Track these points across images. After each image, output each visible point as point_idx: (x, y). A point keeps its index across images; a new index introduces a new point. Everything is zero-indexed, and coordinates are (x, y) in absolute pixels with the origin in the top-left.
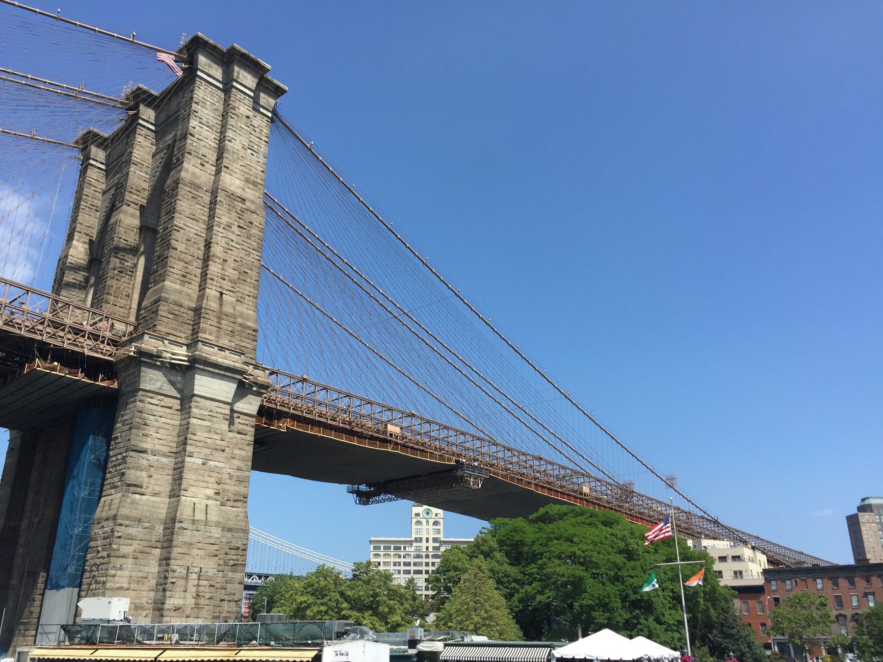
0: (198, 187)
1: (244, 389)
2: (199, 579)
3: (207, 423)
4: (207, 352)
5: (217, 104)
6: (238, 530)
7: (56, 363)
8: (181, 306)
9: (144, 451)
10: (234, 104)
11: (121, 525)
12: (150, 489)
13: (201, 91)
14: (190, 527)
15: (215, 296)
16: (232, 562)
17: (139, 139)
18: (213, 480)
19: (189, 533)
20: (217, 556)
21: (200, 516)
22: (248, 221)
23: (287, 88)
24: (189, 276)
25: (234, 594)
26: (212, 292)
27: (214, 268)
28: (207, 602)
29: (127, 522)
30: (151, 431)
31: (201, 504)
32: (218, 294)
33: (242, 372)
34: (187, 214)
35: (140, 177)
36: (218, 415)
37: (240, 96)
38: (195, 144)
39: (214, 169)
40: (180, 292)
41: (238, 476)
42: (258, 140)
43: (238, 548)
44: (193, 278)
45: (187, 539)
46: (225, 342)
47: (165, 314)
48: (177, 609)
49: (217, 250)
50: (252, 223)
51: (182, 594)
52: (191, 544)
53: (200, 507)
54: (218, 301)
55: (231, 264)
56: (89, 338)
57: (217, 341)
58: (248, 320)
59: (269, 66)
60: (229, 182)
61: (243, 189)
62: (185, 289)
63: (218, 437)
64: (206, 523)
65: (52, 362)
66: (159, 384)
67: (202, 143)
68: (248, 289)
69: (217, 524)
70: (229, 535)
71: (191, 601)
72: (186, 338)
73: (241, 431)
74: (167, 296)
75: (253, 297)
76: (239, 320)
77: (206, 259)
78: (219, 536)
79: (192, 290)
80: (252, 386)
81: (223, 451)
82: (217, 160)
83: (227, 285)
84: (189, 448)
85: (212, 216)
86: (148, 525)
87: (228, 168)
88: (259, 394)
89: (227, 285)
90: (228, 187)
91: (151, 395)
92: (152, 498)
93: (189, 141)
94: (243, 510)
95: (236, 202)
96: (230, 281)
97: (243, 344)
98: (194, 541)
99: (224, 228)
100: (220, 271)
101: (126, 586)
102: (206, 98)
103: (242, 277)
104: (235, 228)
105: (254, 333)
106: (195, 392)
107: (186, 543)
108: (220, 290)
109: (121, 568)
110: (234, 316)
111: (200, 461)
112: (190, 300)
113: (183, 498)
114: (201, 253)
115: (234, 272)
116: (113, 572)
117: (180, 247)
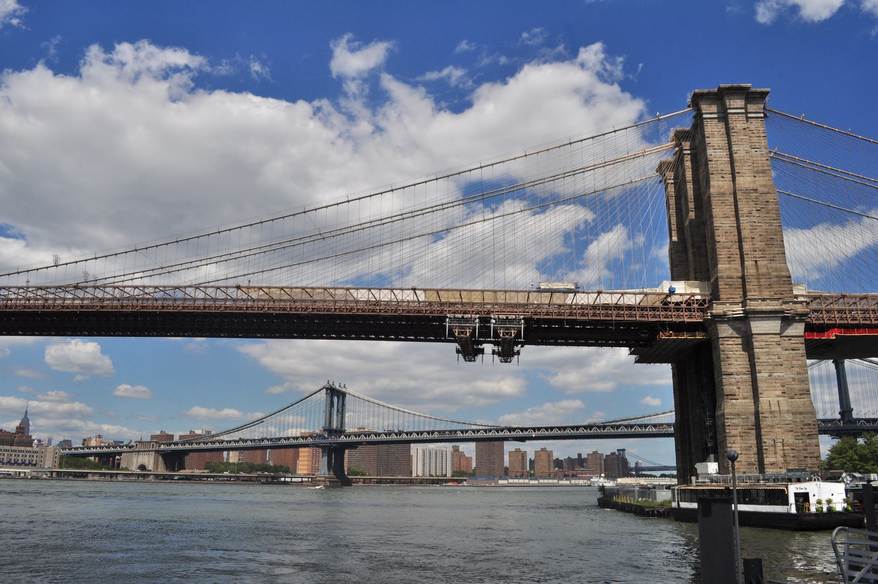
0: (723, 194)
1: (787, 320)
2: (783, 446)
3: (767, 350)
4: (753, 305)
5: (722, 130)
6: (807, 413)
7: (671, 332)
8: (732, 278)
11: (728, 419)
12: (741, 396)
13: (709, 127)
14: (769, 415)
15: (752, 265)
16: (807, 433)
18: (779, 385)
20: (792, 431)
22: (764, 201)
23: (769, 89)
24: (732, 256)
25: (814, 453)
26: (749, 263)
27: (747, 246)
28: (792, 459)
29: (732, 417)
30: (732, 361)
31: (774, 400)
32: (754, 263)
33: (782, 312)
34: (721, 216)
36: (772, 343)
40: (730, 269)
41: (799, 379)
42: (757, 138)
43: (810, 424)
44: (736, 256)
45: (769, 423)
46: (766, 294)
47: (724, 286)
48: (772, 464)
49: (745, 233)
50: (768, 202)
51: (774, 455)
52: (773, 426)
55: (758, 238)
56: (686, 311)
59: (749, 85)
60: (742, 183)
61: (754, 182)
63: (776, 357)
64: (780, 412)
65: (669, 332)
67: (718, 162)
68: (777, 249)
69: (788, 412)
71: (781, 459)
73: (794, 348)
74: (721, 274)
75: (781, 253)
77: (740, 241)
78: (791, 419)
79: (737, 265)
80: (795, 317)
81: (782, 365)
83: (758, 254)
86: (744, 417)
87: (739, 173)
88: (800, 321)
89: (758, 254)
91: (728, 339)
92: (743, 401)
94: (808, 399)
95: (751, 194)
96: (760, 250)
97: (782, 289)
98: (774, 424)
99: (747, 216)
100: (752, 246)
102: (713, 130)
103: (769, 243)
104: (755, 213)
105: (788, 279)
106: (753, 332)
107: (769, 426)
108: (755, 259)
109: (734, 443)
111: (767, 375)
112: (737, 272)
113: (761, 399)
115: (762, 243)
116: (730, 445)
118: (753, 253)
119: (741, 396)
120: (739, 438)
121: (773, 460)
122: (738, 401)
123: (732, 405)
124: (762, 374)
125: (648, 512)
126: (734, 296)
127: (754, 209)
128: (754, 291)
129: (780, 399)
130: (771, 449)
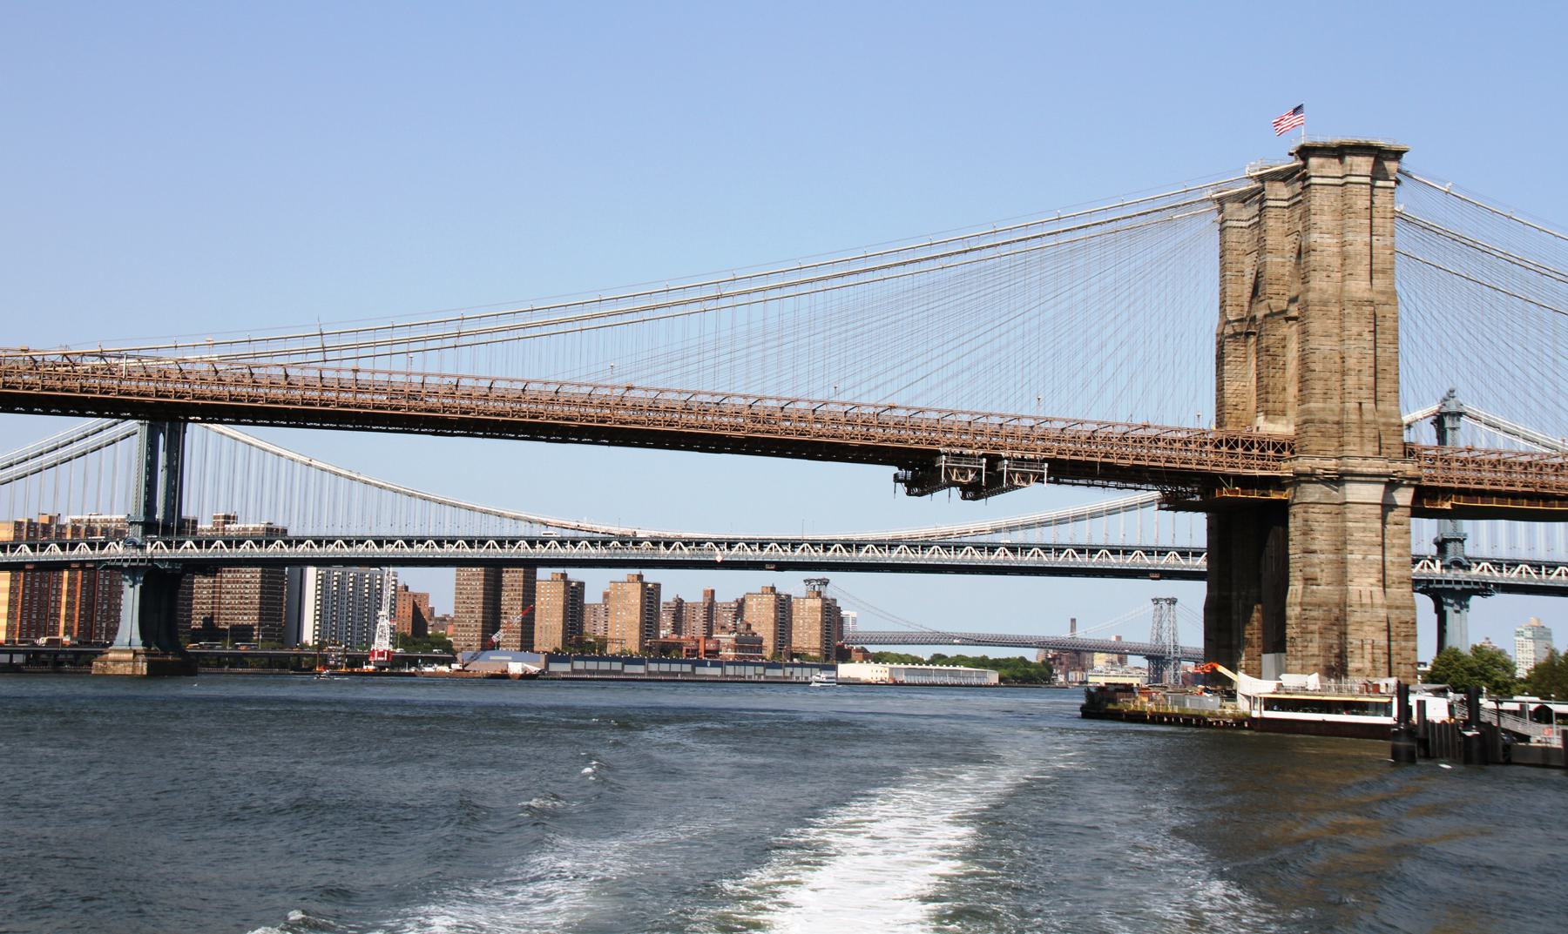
0: (1325, 303)
1: (1392, 484)
3: (1362, 525)
5: (1335, 204)
6: (1405, 608)
9: (1314, 552)
10: (1352, 202)
12: (1324, 580)
16: (1403, 634)
17: (1271, 223)
18: (1373, 570)
19: (1359, 614)
21: (1366, 600)
27: (1351, 381)
29: (1310, 608)
31: (1366, 591)
32: (1357, 405)
34: (1320, 333)
35: (1277, 264)
37: (1356, 188)
38: (1318, 258)
39: (1339, 275)
40: (1323, 409)
42: (1381, 220)
43: (1407, 622)
48: (1358, 670)
49: (1351, 362)
53: (1366, 593)
54: (1357, 412)
57: (1362, 450)
58: (1391, 417)
62: (1328, 405)
64: (1372, 605)
65: (1234, 486)
66: (1317, 495)
67: (1325, 253)
68: (1388, 385)
69: (1382, 606)
70: (1398, 612)
71: (1368, 665)
72: (1335, 450)
74: (1313, 417)
76: (1383, 420)
77: (1344, 373)
79: (1334, 403)
82: (1342, 265)
84: (1349, 547)
85: (1342, 329)
88: (1409, 486)
90: (1354, 295)
93: (1312, 258)
96: (1368, 388)
97: (1388, 442)
98: (1364, 620)
101: (1317, 653)
109: (1311, 641)
110: (1375, 422)
111: (1360, 557)
112: (1334, 415)
114: (1337, 367)
117: (1317, 367)
118: (1357, 391)
119: (1324, 580)
120: (1317, 636)
121: (1359, 665)
122: (1320, 587)
123: (1312, 592)
124: (1353, 556)
125: (1212, 723)
126: (1328, 448)
127: (1367, 329)
128: (1354, 445)
129: (1374, 589)
130: (1359, 651)
